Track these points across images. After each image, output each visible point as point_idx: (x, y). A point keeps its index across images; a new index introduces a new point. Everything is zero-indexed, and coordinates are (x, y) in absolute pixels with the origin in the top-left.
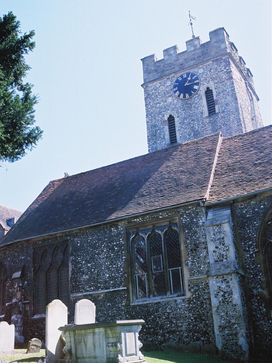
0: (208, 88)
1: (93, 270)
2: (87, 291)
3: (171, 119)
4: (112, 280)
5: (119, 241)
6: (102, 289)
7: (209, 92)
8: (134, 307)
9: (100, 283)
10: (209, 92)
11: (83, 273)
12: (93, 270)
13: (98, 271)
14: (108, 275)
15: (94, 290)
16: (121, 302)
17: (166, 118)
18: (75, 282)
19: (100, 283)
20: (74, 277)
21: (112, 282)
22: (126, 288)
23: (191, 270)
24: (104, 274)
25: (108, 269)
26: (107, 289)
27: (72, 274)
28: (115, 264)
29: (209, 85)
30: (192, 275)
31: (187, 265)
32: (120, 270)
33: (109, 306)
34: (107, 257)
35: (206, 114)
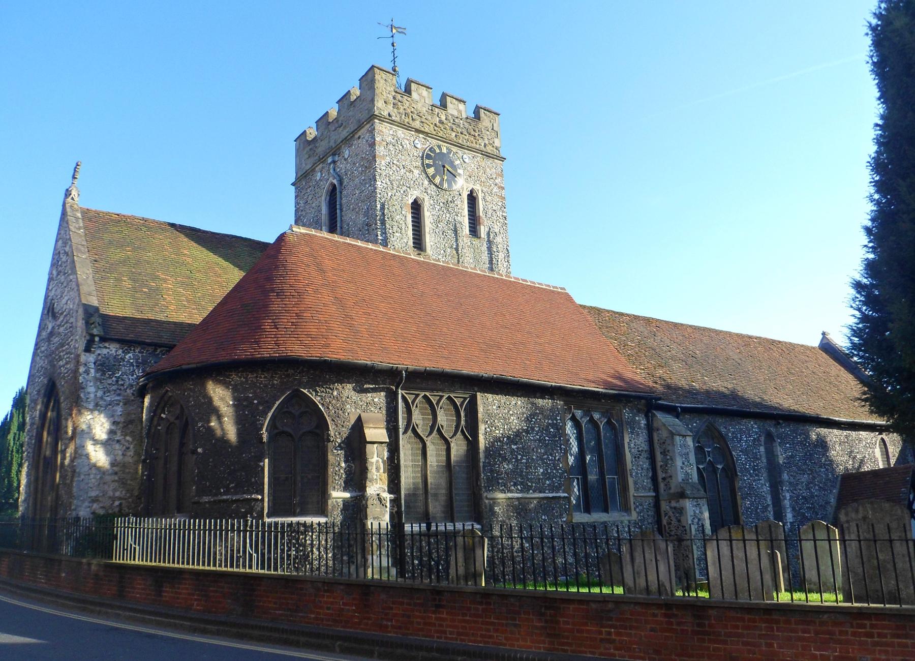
0: (472, 191)
1: (519, 457)
2: (511, 492)
3: (416, 207)
4: (548, 479)
5: (557, 420)
6: (534, 491)
7: (472, 199)
8: (578, 524)
9: (531, 480)
10: (472, 199)
11: (504, 459)
12: (519, 457)
13: (527, 460)
14: (541, 470)
15: (521, 491)
16: (561, 516)
17: (411, 201)
18: (492, 471)
19: (531, 480)
20: (489, 463)
21: (548, 482)
22: (566, 495)
23: (635, 483)
24: (536, 468)
25: (542, 460)
26: (540, 492)
27: (486, 457)
28: (551, 455)
29: (474, 187)
30: (637, 490)
31: (631, 475)
32: (558, 465)
33: (545, 520)
34: (540, 440)
35: (467, 230)
